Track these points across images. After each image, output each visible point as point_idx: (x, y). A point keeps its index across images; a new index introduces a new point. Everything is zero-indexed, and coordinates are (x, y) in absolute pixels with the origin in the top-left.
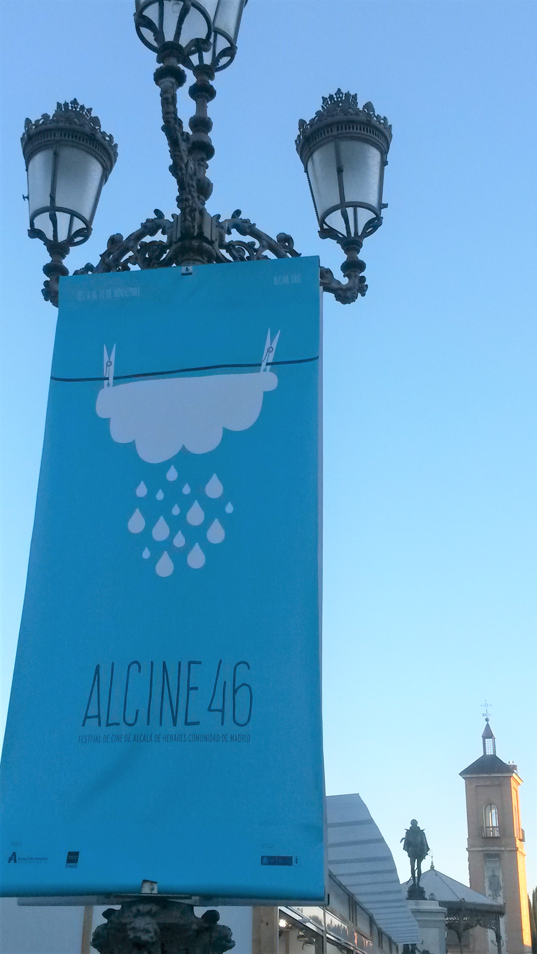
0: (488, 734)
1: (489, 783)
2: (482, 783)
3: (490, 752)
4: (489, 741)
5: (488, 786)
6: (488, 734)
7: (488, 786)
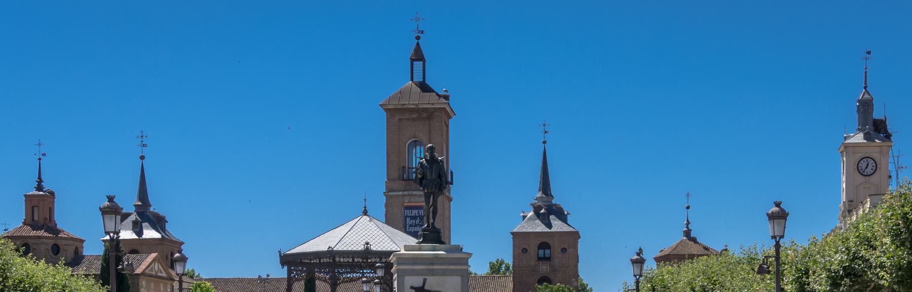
0: (418, 56)
1: (414, 116)
2: (407, 116)
3: (418, 78)
4: (418, 65)
5: (414, 120)
6: (418, 56)
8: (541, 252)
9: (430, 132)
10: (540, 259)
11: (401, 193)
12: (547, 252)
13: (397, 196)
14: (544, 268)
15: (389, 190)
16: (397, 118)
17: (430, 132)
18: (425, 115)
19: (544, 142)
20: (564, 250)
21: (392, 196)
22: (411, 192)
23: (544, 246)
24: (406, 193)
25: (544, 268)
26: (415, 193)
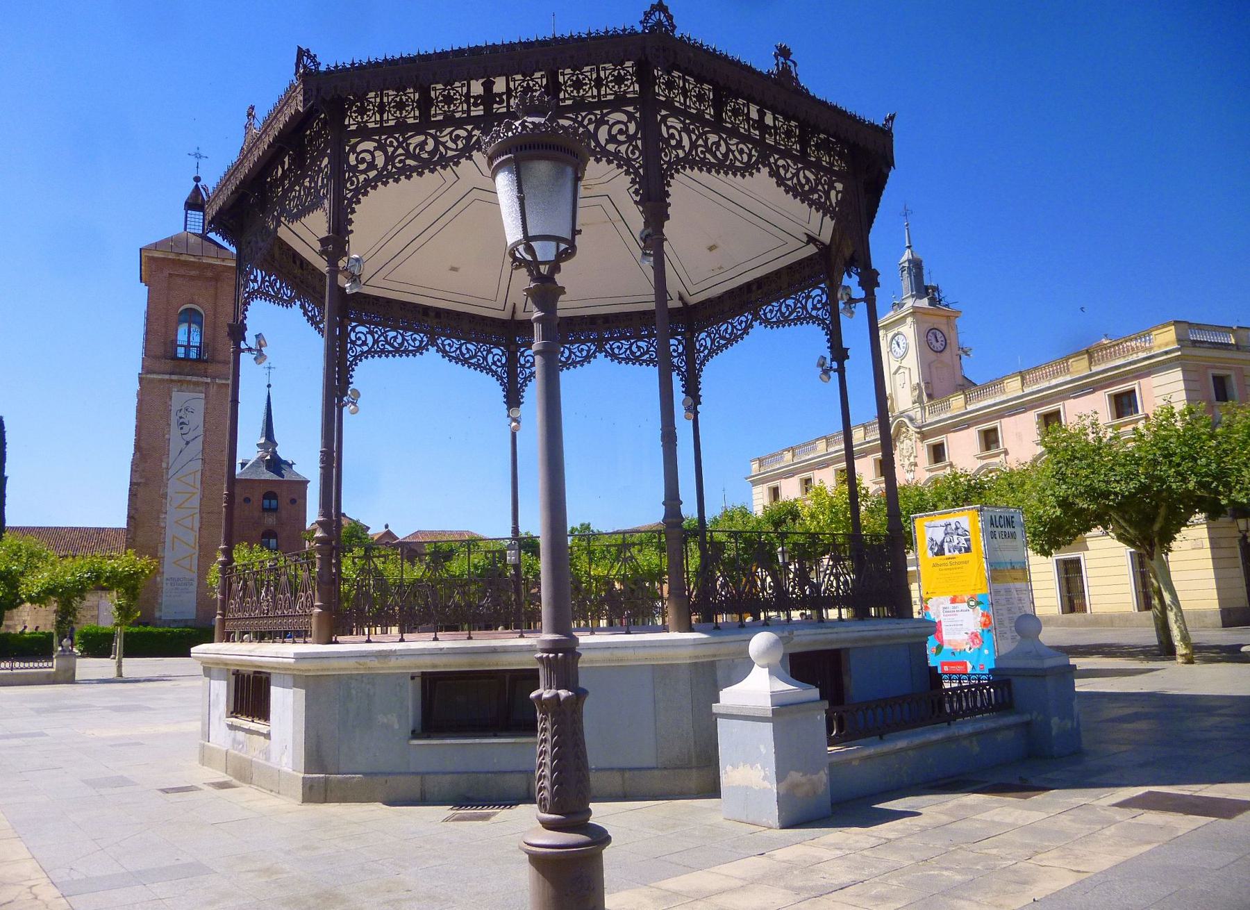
1: (192, 273)
2: (182, 271)
5: (192, 278)
7: (192, 278)
8: (266, 502)
9: (216, 297)
10: (264, 510)
11: (167, 377)
12: (274, 502)
13: (163, 380)
14: (270, 520)
15: (146, 369)
16: (166, 272)
17: (216, 297)
18: (209, 274)
19: (269, 386)
20: (293, 501)
21: (151, 381)
22: (182, 378)
23: (270, 495)
24: (174, 377)
25: (270, 520)
26: (189, 378)
